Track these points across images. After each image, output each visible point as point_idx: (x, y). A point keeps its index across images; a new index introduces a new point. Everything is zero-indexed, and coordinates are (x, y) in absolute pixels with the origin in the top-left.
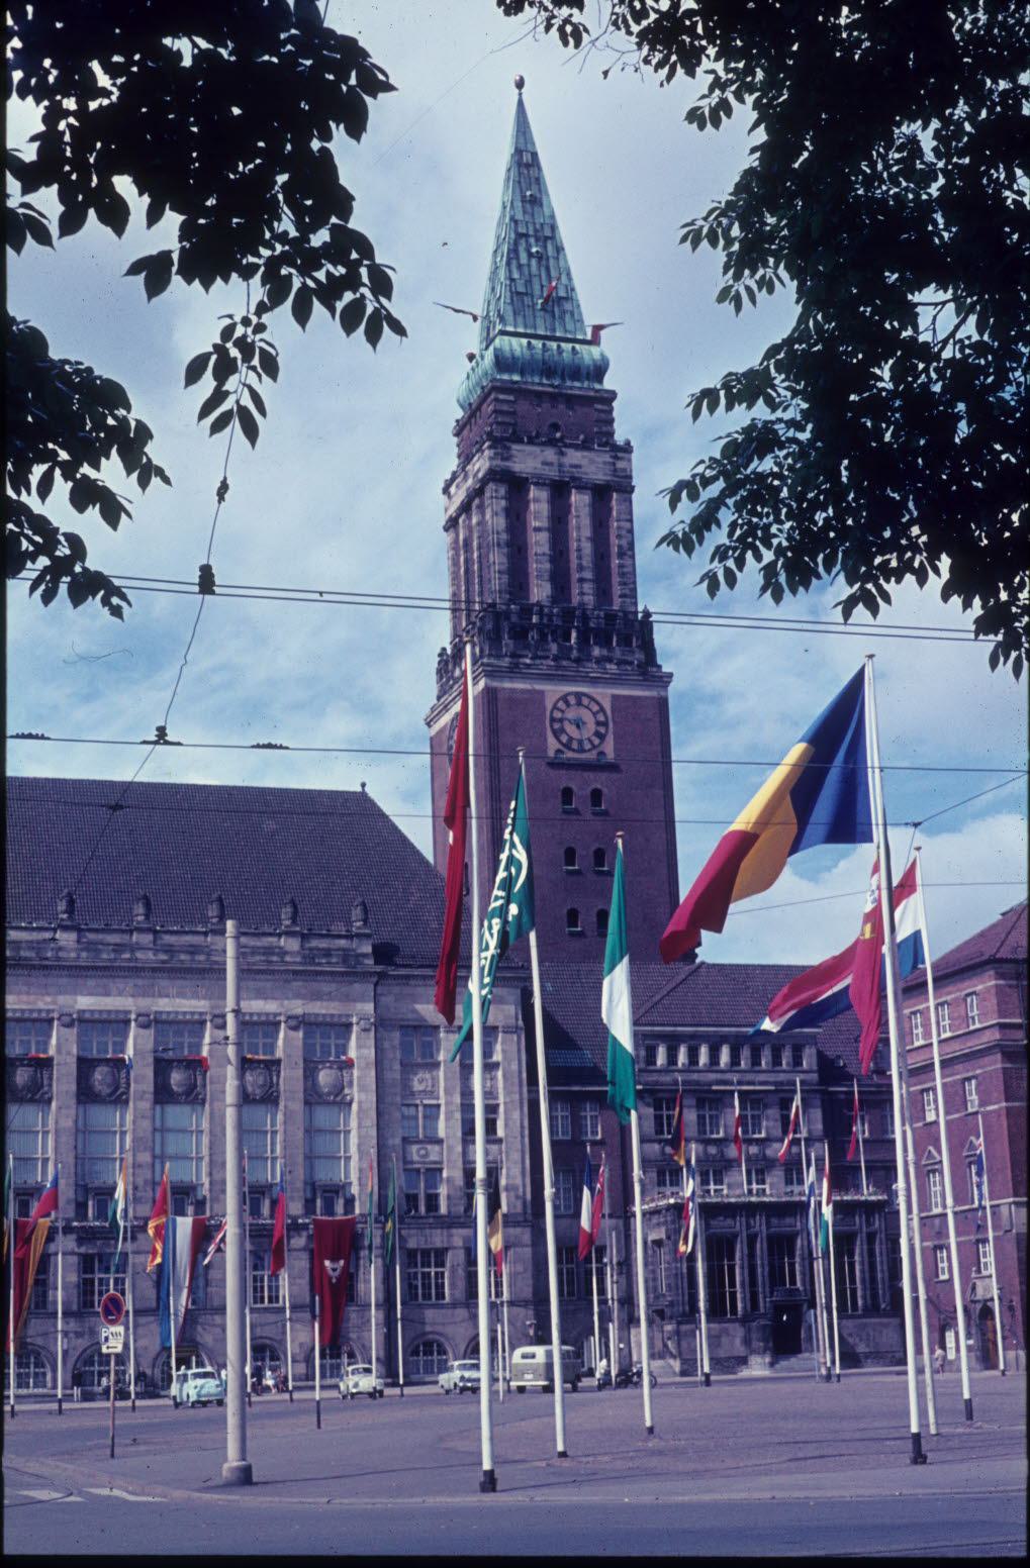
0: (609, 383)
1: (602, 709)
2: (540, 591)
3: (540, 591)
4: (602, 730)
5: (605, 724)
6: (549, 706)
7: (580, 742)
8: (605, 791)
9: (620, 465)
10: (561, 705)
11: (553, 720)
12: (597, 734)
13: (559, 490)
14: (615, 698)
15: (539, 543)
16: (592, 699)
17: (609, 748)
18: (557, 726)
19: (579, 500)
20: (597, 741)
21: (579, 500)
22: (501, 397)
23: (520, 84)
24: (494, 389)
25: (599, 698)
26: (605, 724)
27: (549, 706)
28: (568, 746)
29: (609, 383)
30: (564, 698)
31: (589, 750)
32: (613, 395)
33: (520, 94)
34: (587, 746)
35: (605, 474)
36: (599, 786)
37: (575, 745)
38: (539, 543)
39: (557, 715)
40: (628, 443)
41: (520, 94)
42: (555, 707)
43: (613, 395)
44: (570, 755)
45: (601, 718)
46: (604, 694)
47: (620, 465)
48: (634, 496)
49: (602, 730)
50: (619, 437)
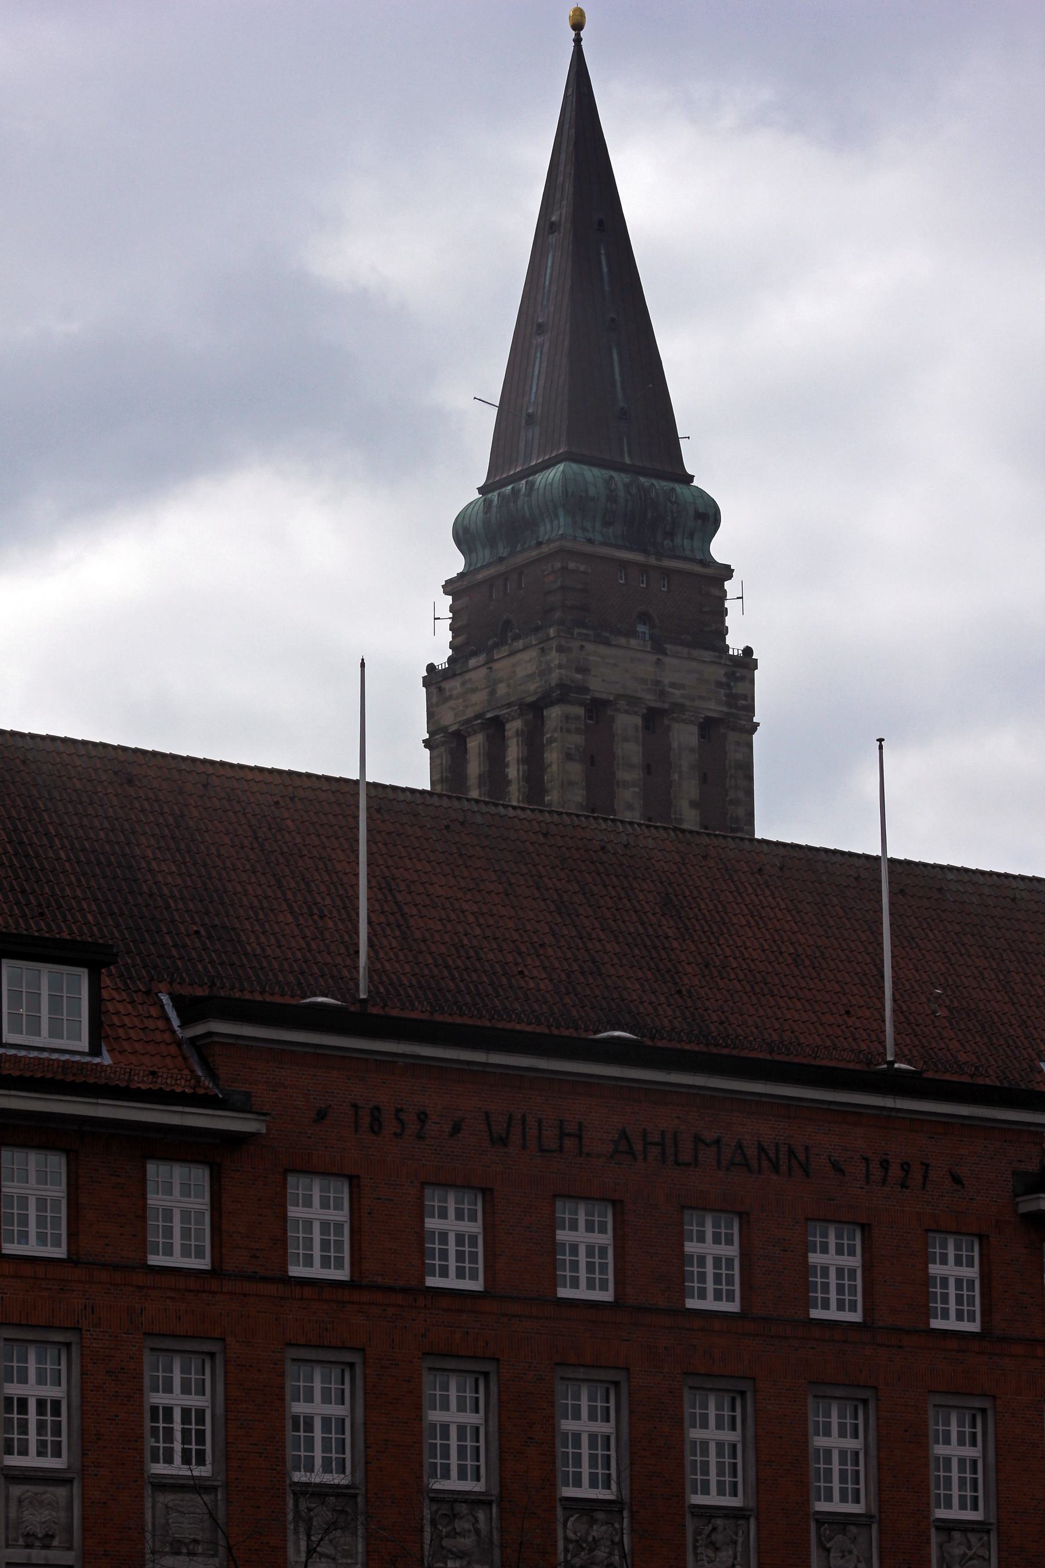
0: (720, 549)
22: (572, 565)
23: (578, 26)
24: (561, 551)
29: (720, 549)
32: (727, 572)
33: (578, 41)
40: (748, 651)
41: (578, 41)
43: (727, 572)
48: (756, 737)
50: (735, 643)
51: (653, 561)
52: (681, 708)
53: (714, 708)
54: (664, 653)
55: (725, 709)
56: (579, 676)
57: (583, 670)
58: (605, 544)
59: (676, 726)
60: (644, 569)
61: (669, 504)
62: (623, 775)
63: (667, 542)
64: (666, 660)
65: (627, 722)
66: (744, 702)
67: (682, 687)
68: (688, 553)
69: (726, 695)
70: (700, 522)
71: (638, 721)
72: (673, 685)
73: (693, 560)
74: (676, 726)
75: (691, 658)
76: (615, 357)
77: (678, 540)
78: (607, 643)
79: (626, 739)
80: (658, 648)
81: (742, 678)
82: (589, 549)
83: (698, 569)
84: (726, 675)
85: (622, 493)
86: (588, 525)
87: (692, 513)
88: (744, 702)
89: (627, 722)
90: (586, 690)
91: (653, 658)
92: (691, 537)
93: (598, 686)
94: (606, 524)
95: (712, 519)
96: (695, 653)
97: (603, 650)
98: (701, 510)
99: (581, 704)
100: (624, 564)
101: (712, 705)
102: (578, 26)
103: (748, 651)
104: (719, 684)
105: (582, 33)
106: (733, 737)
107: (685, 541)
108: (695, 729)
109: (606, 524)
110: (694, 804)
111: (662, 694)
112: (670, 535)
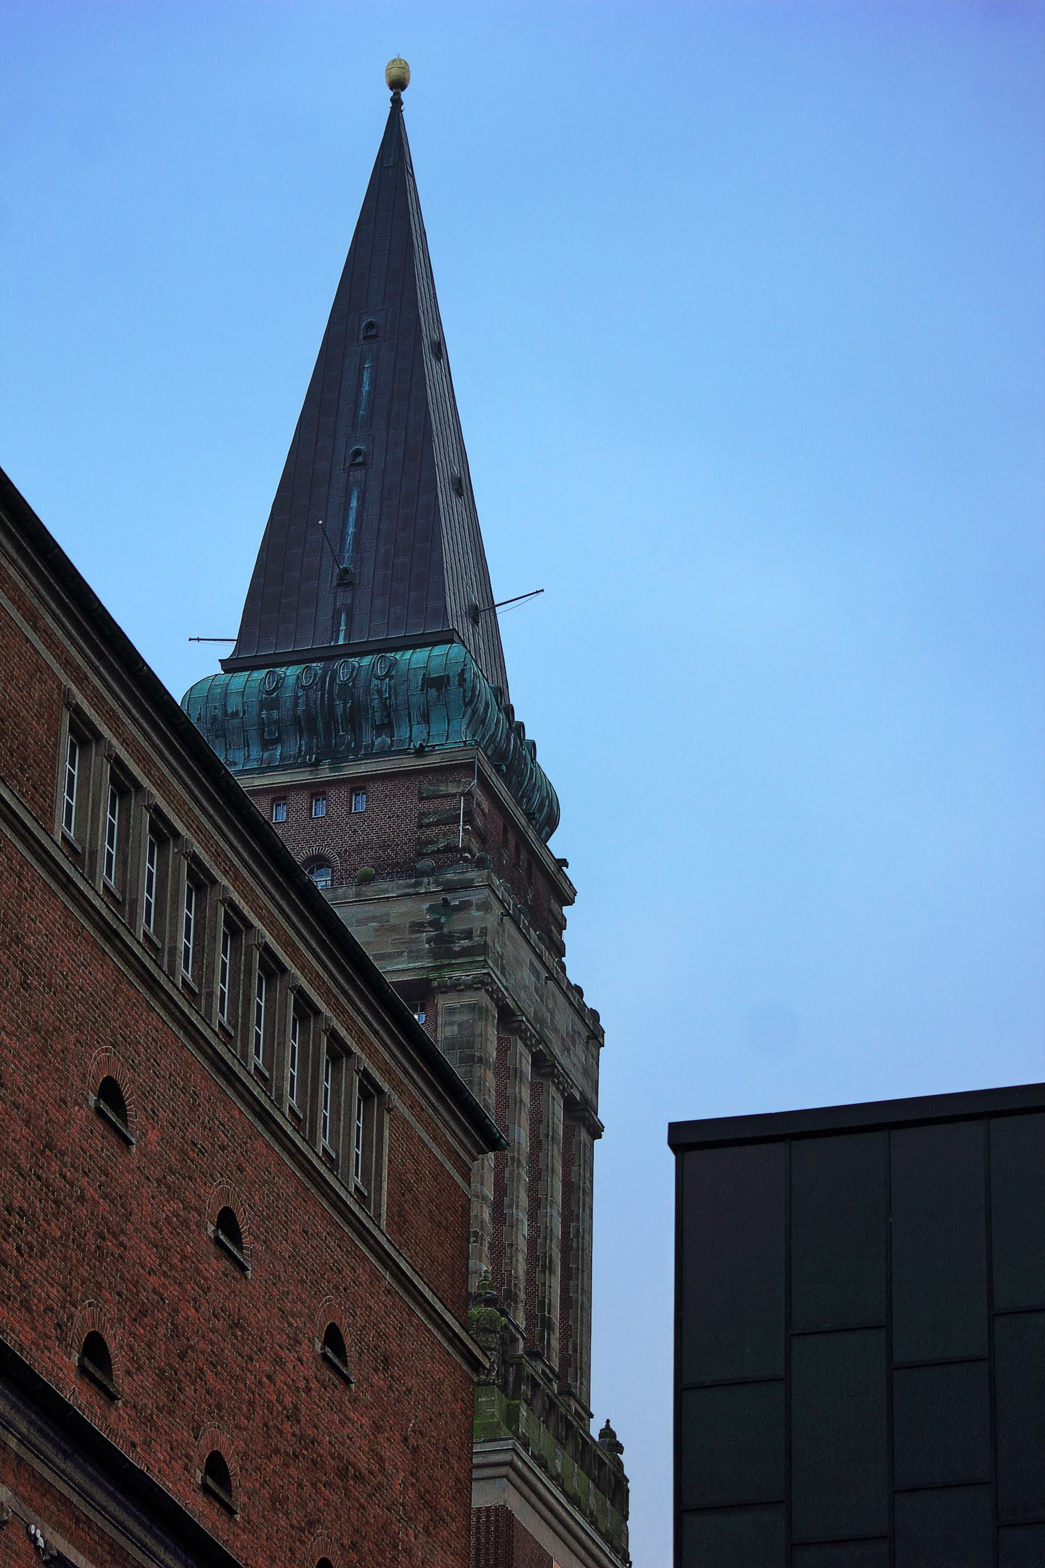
23: (398, 84)
33: (397, 103)
35: (414, 956)
41: (397, 103)
51: (325, 773)
55: (427, 963)
61: (375, 682)
66: (465, 943)
69: (428, 941)
70: (433, 693)
76: (354, 504)
77: (402, 732)
83: (410, 763)
84: (431, 910)
88: (465, 943)
92: (426, 719)
94: (266, 744)
95: (454, 681)
96: (369, 891)
102: (398, 84)
104: (417, 927)
105: (404, 95)
107: (415, 728)
109: (266, 744)
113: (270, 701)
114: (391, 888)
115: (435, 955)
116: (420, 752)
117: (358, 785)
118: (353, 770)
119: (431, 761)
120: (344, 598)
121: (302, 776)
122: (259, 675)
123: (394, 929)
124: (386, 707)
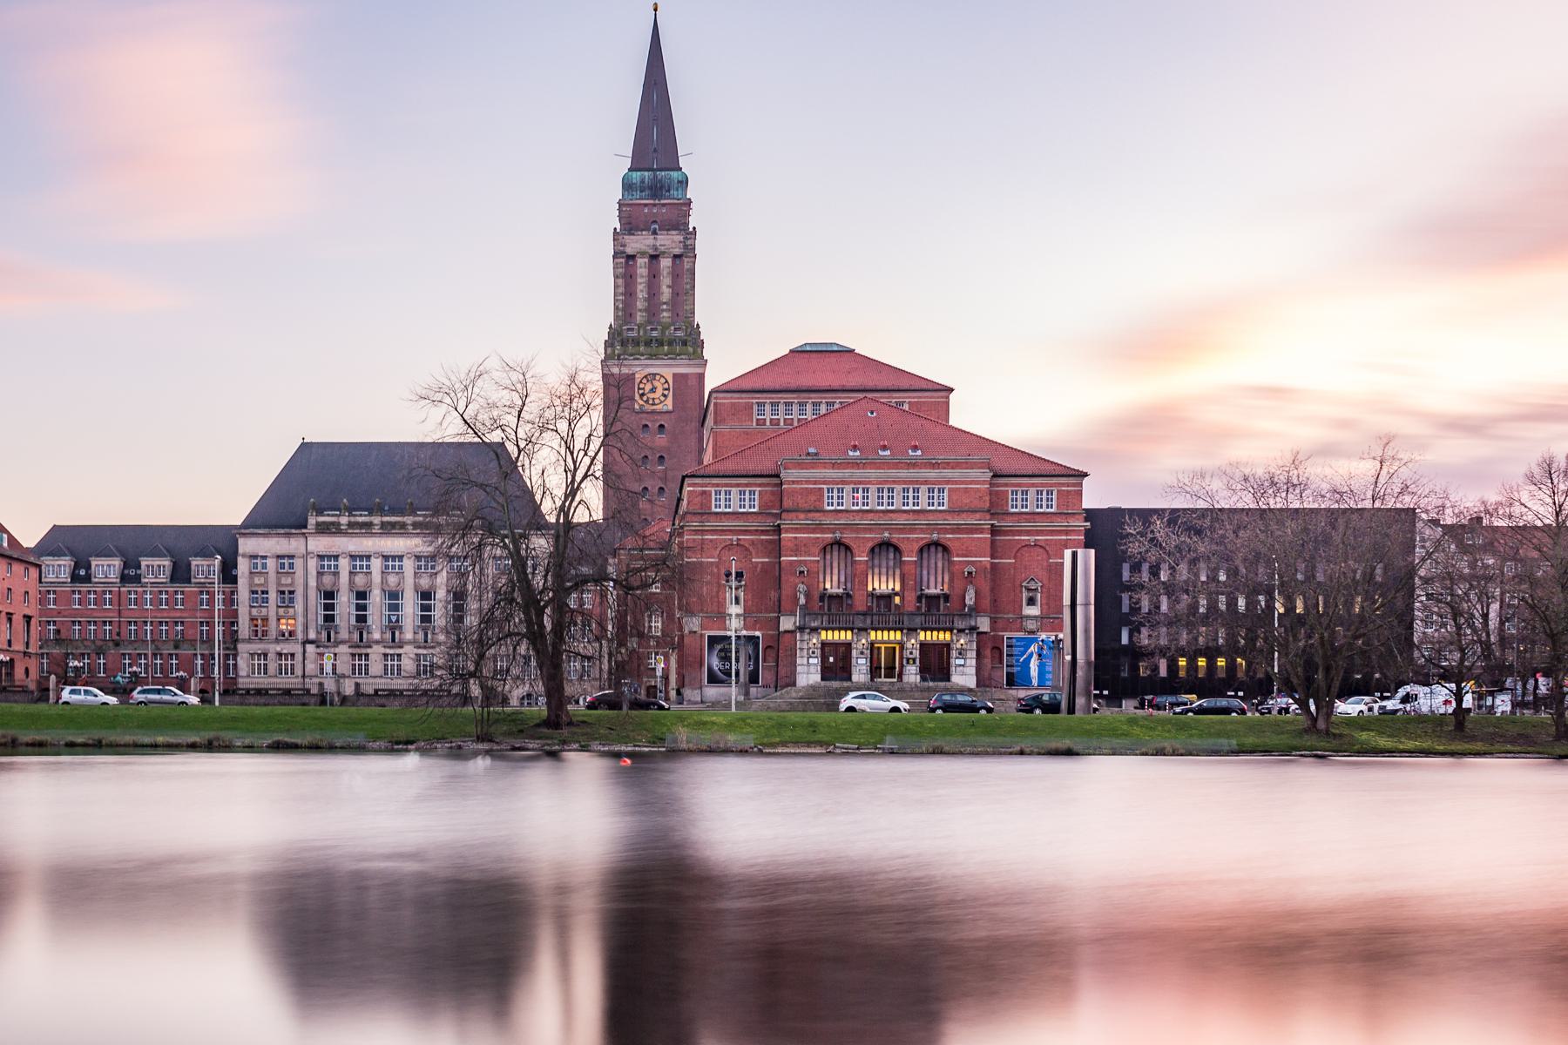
1: (667, 382)
2: (640, 317)
3: (640, 317)
4: (666, 392)
5: (668, 389)
6: (637, 381)
7: (653, 399)
8: (666, 425)
9: (689, 242)
10: (645, 381)
11: (639, 389)
12: (665, 396)
13: (654, 258)
14: (675, 375)
15: (641, 292)
16: (662, 376)
17: (669, 404)
18: (641, 392)
19: (665, 263)
20: (662, 398)
21: (665, 263)
25: (664, 375)
26: (668, 389)
27: (637, 381)
28: (647, 402)
30: (646, 377)
31: (658, 404)
34: (657, 401)
35: (681, 248)
36: (663, 423)
37: (651, 402)
38: (641, 292)
39: (641, 386)
40: (694, 228)
42: (641, 382)
44: (649, 408)
45: (666, 386)
46: (668, 373)
47: (689, 242)
49: (666, 392)
51: (657, 202)
52: (664, 253)
53: (677, 251)
54: (657, 234)
56: (622, 248)
57: (624, 246)
58: (637, 199)
59: (662, 260)
60: (655, 205)
62: (639, 280)
63: (667, 194)
64: (658, 237)
65: (642, 262)
67: (664, 245)
68: (675, 196)
71: (646, 260)
72: (660, 245)
73: (674, 199)
74: (662, 260)
75: (668, 234)
77: (672, 192)
78: (633, 234)
79: (641, 267)
80: (655, 233)
81: (690, 238)
82: (631, 202)
83: (676, 201)
85: (647, 180)
86: (634, 193)
87: (676, 181)
89: (642, 262)
90: (625, 253)
91: (653, 237)
92: (677, 190)
93: (629, 251)
94: (641, 191)
96: (669, 232)
97: (632, 237)
98: (680, 179)
99: (623, 258)
100: (646, 205)
101: (677, 250)
103: (694, 228)
104: (680, 242)
106: (686, 260)
108: (670, 260)
109: (641, 191)
110: (669, 287)
111: (656, 249)
112: (669, 191)
113: (642, 181)
114: (674, 232)
115: (684, 249)
116: (678, 200)
117: (664, 205)
118: (662, 202)
119: (681, 201)
120: (655, 155)
121: (652, 202)
122: (639, 173)
123: (675, 242)
124: (669, 186)
